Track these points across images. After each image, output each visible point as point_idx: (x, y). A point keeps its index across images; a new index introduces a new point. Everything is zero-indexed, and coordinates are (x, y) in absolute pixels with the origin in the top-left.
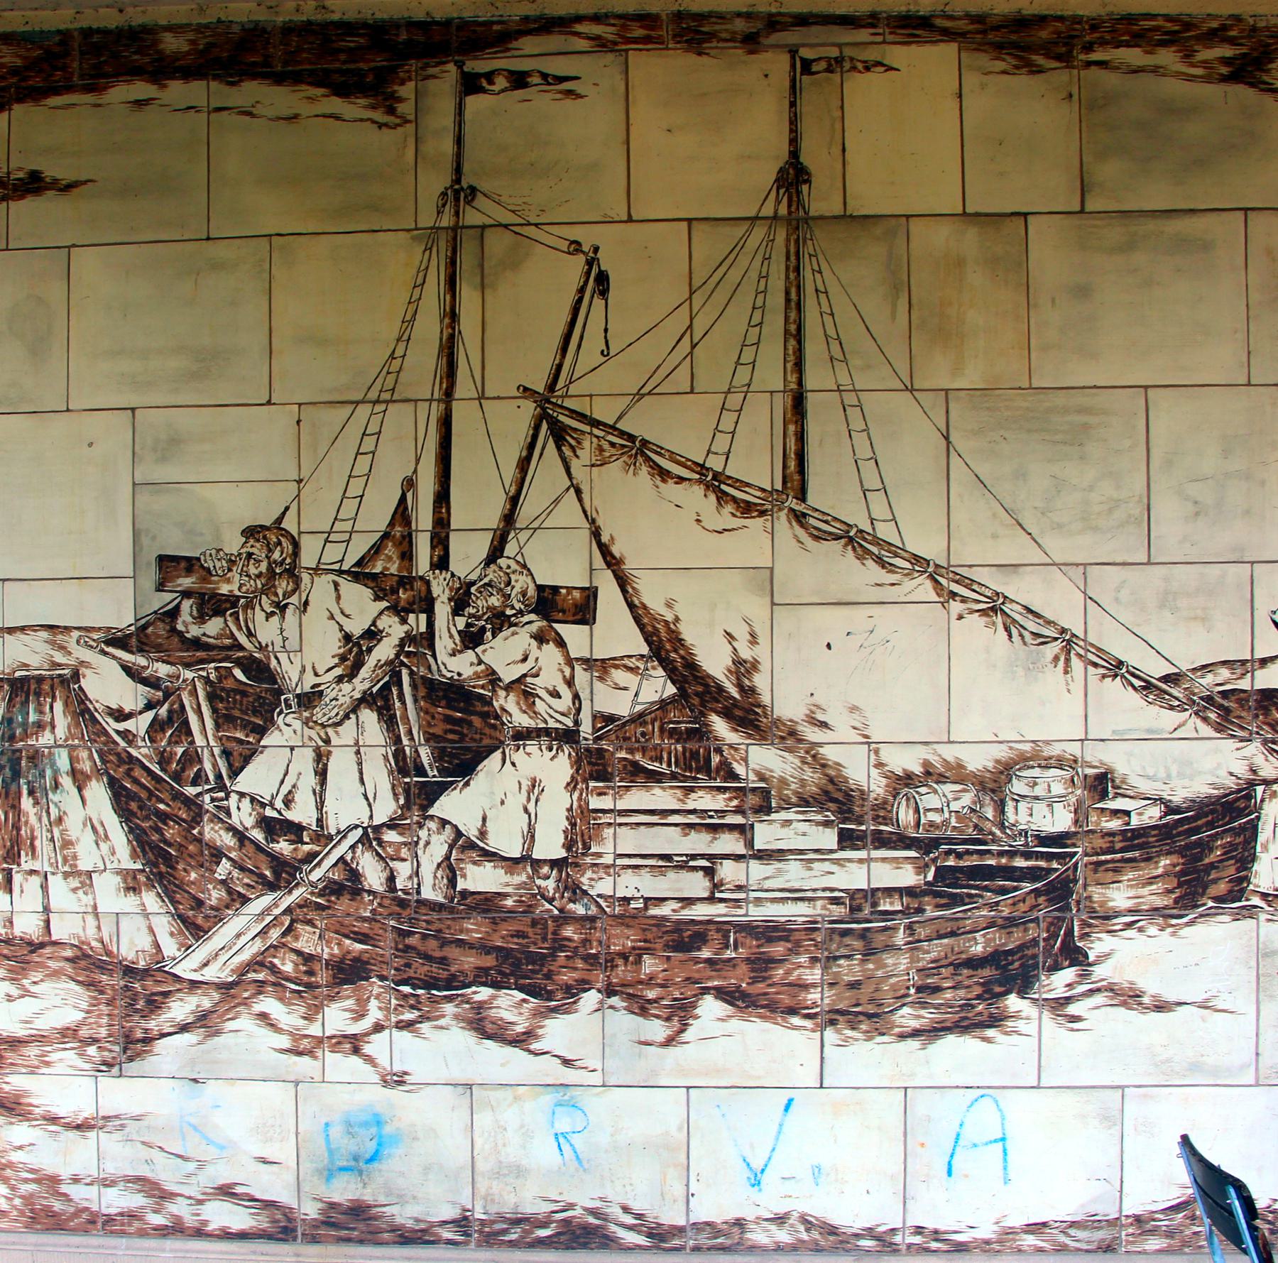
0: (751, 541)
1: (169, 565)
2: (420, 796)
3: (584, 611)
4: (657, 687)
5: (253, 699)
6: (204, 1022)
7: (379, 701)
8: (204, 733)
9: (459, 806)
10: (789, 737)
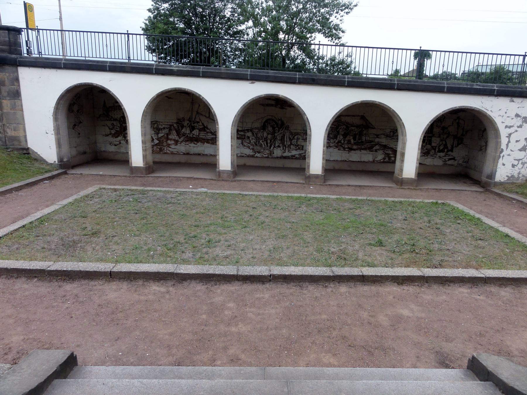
1: (178, 119)
2: (191, 132)
3: (199, 122)
5: (183, 127)
7: (189, 127)
8: (180, 128)
9: (193, 132)
10: (209, 129)
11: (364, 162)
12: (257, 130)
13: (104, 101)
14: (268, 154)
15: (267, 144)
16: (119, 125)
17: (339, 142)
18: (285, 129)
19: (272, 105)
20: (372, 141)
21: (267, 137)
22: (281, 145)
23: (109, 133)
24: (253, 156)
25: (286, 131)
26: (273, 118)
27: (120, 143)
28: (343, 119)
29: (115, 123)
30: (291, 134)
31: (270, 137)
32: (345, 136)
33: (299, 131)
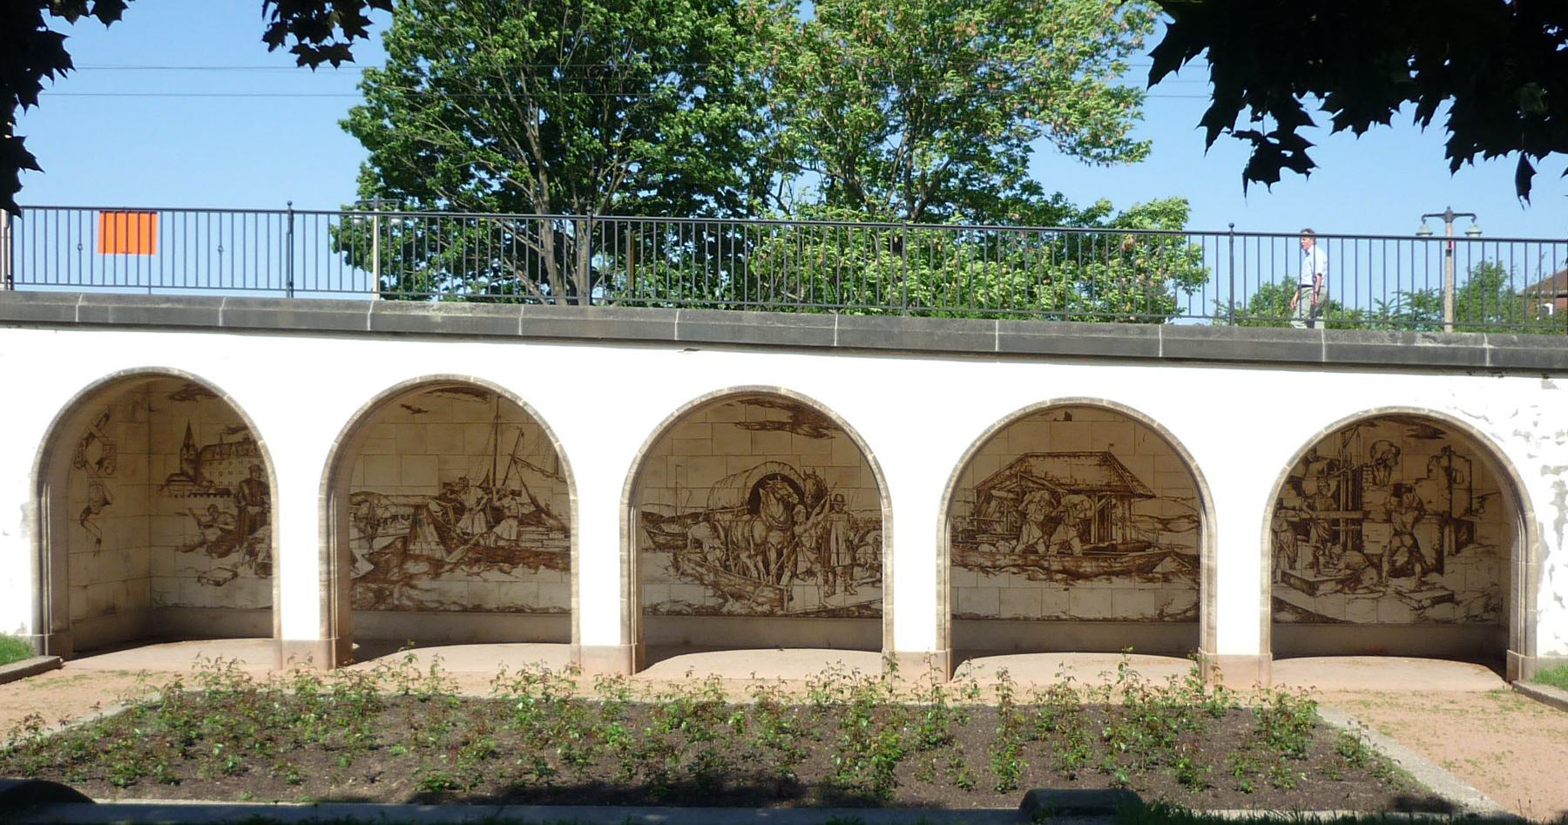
0: (550, 482)
1: (445, 485)
2: (490, 528)
4: (533, 508)
5: (460, 510)
6: (451, 570)
7: (483, 510)
9: (498, 530)
10: (555, 518)
11: (1126, 620)
12: (729, 517)
13: (189, 428)
14: (771, 600)
15: (766, 564)
16: (235, 512)
17: (1031, 549)
18: (832, 507)
19: (780, 426)
20: (1149, 545)
21: (765, 541)
22: (817, 568)
23: (197, 540)
24: (715, 612)
25: (834, 516)
26: (786, 472)
27: (235, 575)
28: (1039, 468)
29: (220, 503)
30: (854, 525)
31: (775, 537)
32: (1050, 525)
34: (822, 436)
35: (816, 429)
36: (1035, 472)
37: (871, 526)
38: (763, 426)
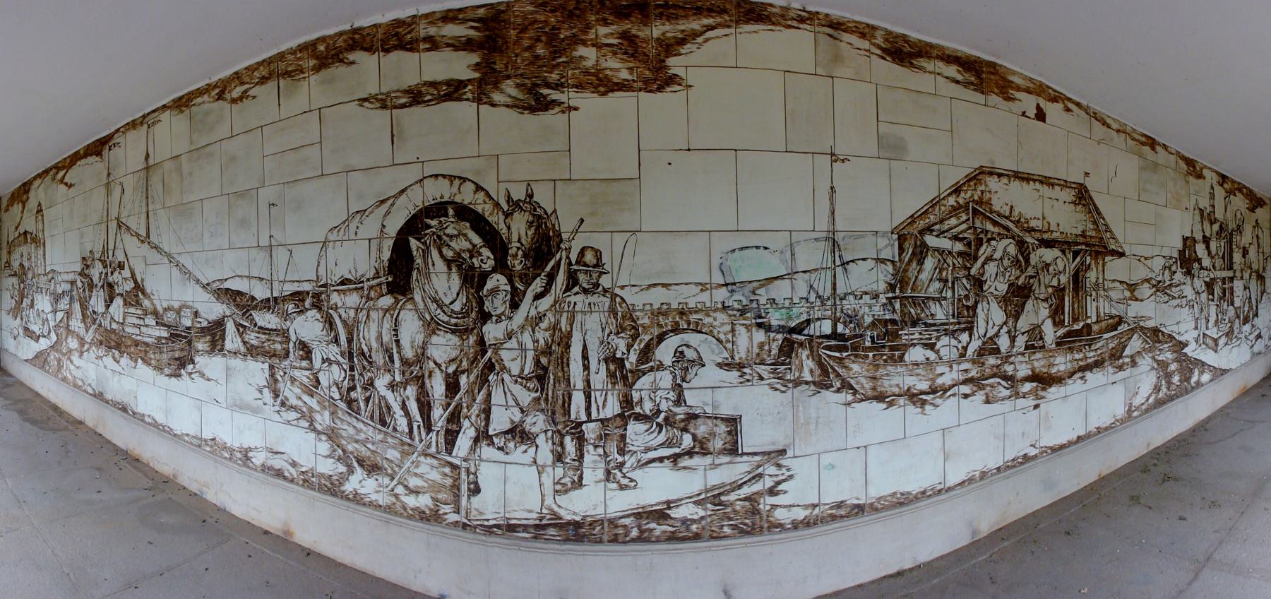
12: (353, 299)
18: (572, 281)
19: (452, 91)
21: (422, 356)
25: (580, 300)
26: (466, 196)
30: (626, 322)
31: (443, 348)
33: (693, 298)
34: (540, 105)
35: (532, 90)
36: (997, 205)
37: (667, 322)
38: (415, 97)
